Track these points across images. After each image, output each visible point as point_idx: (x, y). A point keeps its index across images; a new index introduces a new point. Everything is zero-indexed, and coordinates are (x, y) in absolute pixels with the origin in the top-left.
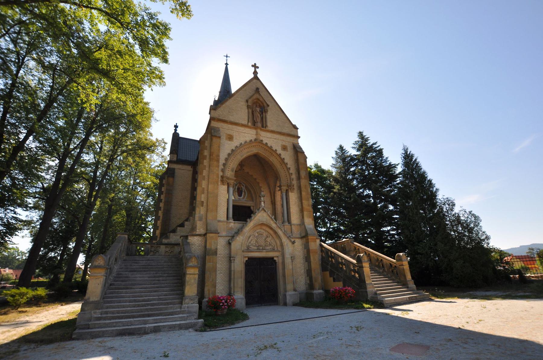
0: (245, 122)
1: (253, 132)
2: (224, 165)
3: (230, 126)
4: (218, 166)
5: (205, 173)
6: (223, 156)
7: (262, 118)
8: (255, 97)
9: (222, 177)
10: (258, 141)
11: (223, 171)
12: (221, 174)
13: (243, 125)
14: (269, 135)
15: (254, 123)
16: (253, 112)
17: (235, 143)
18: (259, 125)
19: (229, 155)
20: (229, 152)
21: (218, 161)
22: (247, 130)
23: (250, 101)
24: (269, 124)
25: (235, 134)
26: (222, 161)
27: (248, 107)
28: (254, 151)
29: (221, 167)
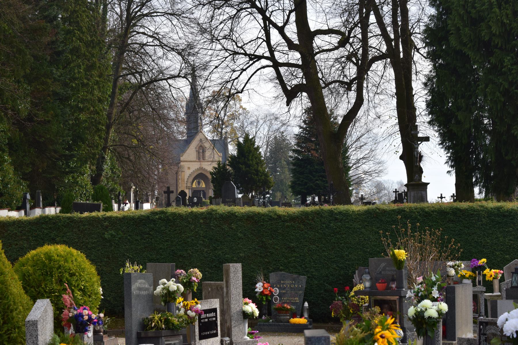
0: (195, 159)
1: (199, 163)
2: (187, 181)
3: (189, 163)
4: (184, 183)
5: (180, 185)
6: (186, 177)
7: (203, 155)
8: (199, 145)
9: (186, 186)
10: (201, 168)
11: (186, 184)
12: (185, 185)
13: (194, 162)
14: (206, 163)
15: (199, 158)
16: (199, 153)
17: (191, 171)
18: (201, 159)
19: (189, 177)
20: (188, 175)
21: (184, 181)
22: (196, 163)
23: (197, 148)
24: (207, 158)
25: (191, 166)
26: (186, 180)
27: (197, 151)
28: (200, 172)
29: (185, 182)
